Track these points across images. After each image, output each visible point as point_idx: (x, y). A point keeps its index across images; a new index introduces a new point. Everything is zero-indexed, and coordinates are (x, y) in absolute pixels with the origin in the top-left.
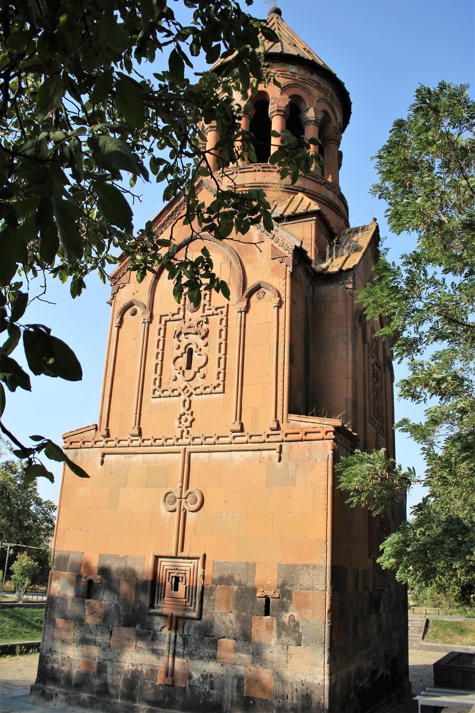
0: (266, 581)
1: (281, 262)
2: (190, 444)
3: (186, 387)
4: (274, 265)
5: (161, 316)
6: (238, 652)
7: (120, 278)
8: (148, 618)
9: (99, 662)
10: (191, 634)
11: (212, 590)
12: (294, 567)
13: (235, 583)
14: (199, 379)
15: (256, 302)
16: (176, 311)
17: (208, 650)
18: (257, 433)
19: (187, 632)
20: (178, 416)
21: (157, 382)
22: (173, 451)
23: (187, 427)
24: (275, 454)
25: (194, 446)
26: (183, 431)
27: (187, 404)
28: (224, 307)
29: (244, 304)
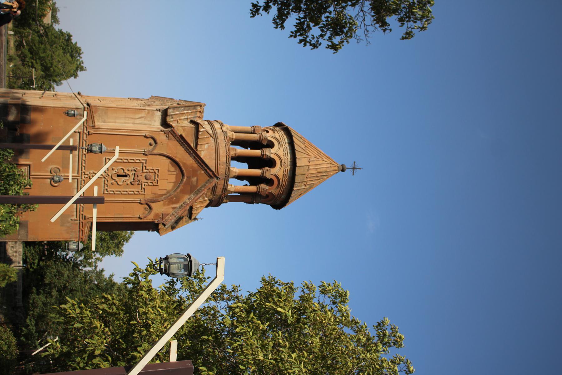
12: (27, 227)
16: (147, 168)
24: (74, 218)
29: (143, 202)
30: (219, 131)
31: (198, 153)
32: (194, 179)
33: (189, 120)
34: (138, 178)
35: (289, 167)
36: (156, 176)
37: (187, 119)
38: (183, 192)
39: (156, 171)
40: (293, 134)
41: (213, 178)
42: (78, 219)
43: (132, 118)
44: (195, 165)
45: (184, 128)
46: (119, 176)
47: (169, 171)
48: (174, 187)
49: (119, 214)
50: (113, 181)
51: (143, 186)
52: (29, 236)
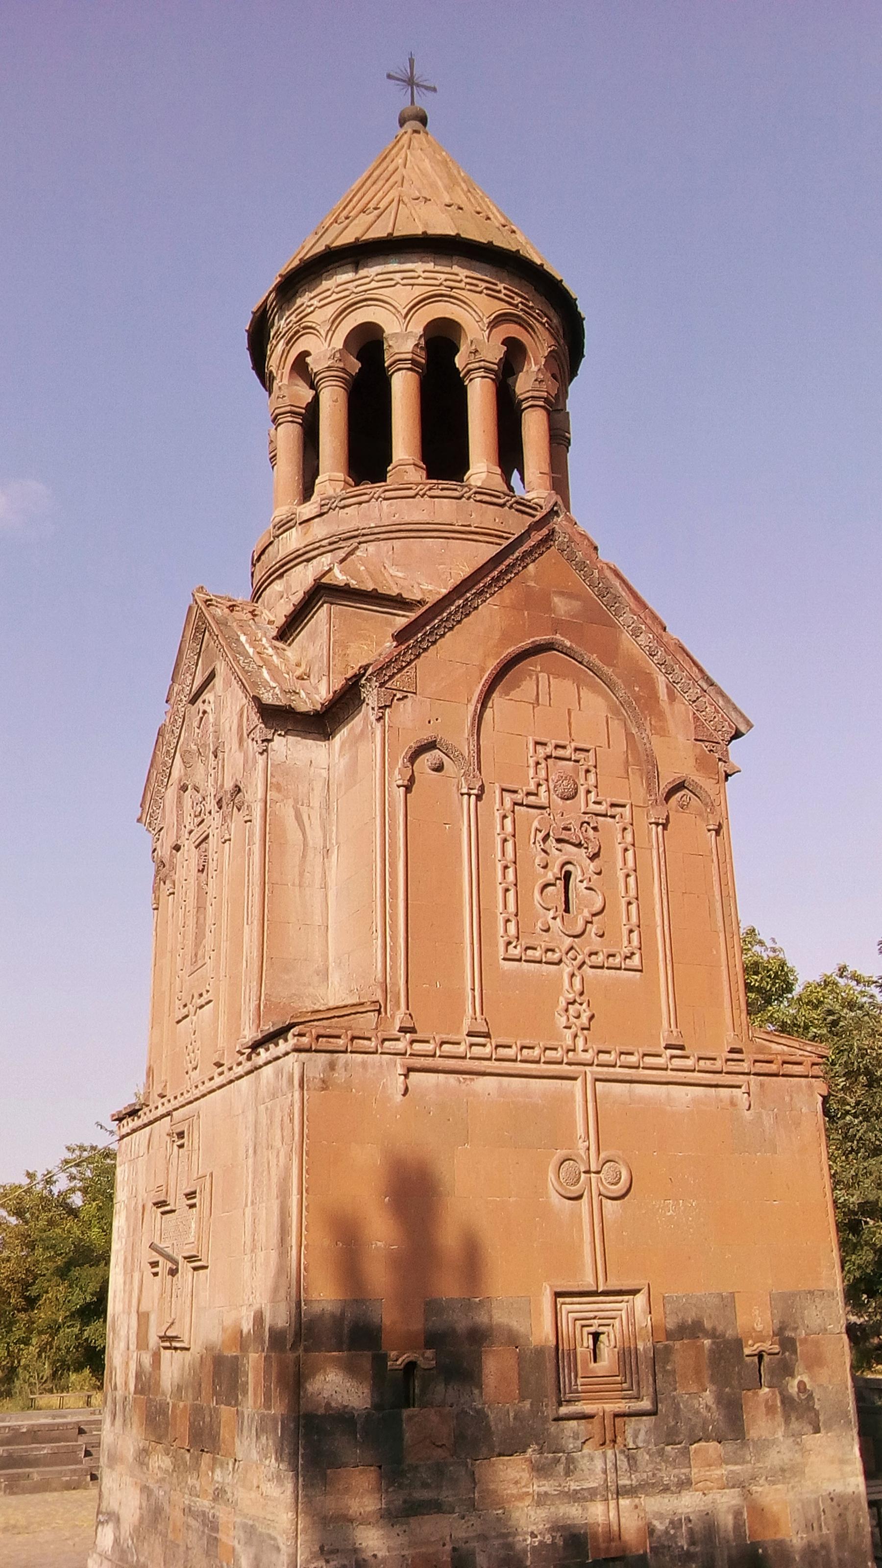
0: (755, 1322)
1: (710, 751)
2: (591, 1065)
3: (572, 948)
4: (698, 751)
5: (503, 790)
6: (727, 1464)
8: (553, 1428)
9: (454, 1549)
10: (640, 1445)
11: (668, 1350)
12: (793, 1295)
13: (707, 1334)
14: (593, 935)
17: (676, 1471)
19: (634, 1442)
20: (564, 1004)
21: (512, 928)
23: (583, 1029)
25: (600, 1069)
27: (577, 981)
28: (624, 806)
30: (319, 530)
31: (432, 600)
34: (575, 826)
35: (456, 269)
36: (560, 753)
37: (275, 648)
38: (610, 653)
40: (320, 248)
41: (553, 531)
43: (304, 856)
44: (507, 594)
45: (337, 647)
46: (567, 910)
50: (593, 929)
51: (601, 809)
52: (825, 1286)
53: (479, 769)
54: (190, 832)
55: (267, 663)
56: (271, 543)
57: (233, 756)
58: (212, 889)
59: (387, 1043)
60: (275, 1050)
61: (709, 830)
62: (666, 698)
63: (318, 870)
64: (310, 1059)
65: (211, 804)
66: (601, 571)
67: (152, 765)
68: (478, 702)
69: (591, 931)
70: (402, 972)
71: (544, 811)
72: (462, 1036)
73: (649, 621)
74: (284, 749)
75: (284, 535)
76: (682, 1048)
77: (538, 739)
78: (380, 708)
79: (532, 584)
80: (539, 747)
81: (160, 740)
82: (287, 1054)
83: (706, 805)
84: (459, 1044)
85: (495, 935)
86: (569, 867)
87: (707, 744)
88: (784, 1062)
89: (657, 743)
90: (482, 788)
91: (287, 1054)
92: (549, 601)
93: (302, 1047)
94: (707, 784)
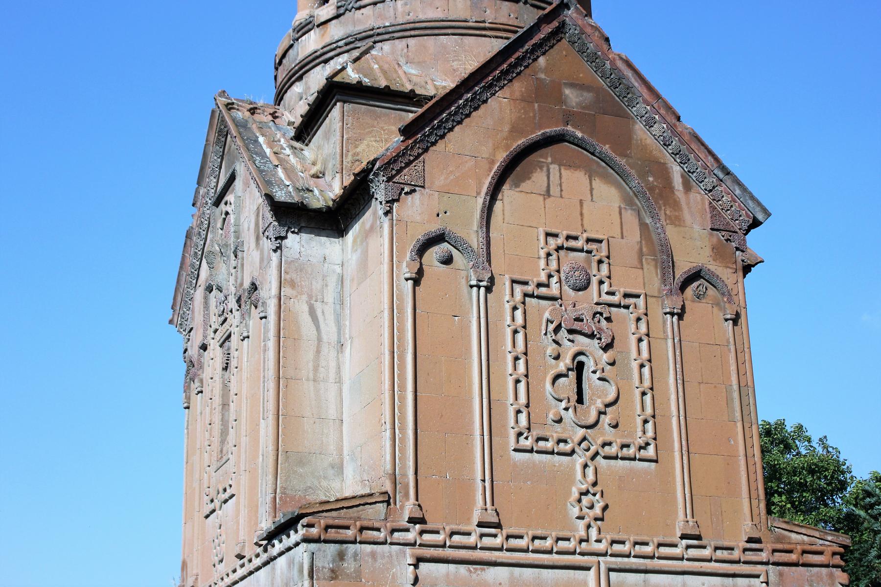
1: (727, 240)
4: (715, 240)
5: (513, 282)
7: (402, 169)
14: (607, 427)
15: (693, 301)
18: (726, 544)
20: (576, 495)
21: (523, 418)
22: (577, 564)
23: (596, 519)
25: (613, 559)
26: (589, 526)
27: (590, 471)
28: (638, 296)
30: (336, 31)
32: (572, 97)
33: (298, 145)
34: (587, 317)
36: (572, 243)
37: (292, 147)
38: (624, 142)
39: (553, 243)
41: (563, 24)
42: (759, 569)
43: (318, 351)
44: (518, 87)
46: (580, 400)
47: (548, 194)
48: (605, 178)
49: (729, 400)
50: (606, 420)
51: (615, 299)
53: (489, 261)
54: (216, 331)
55: (283, 163)
56: (291, 46)
57: (251, 255)
58: (233, 387)
59: (396, 534)
60: (287, 542)
61: (726, 320)
62: (681, 188)
63: (333, 364)
64: (319, 550)
65: (232, 304)
66: (613, 63)
67: (181, 268)
68: (487, 194)
69: (604, 421)
70: (411, 463)
71: (556, 303)
72: (472, 527)
73: (662, 111)
74: (297, 247)
75: (303, 38)
76: (698, 537)
77: (549, 230)
78: (387, 202)
79: (542, 76)
80: (551, 240)
81: (188, 243)
82: (297, 544)
83: (723, 294)
84: (469, 534)
85: (504, 426)
86: (581, 358)
87: (723, 233)
88: (804, 552)
89: (672, 233)
90: (492, 280)
91: (297, 544)
92: (560, 93)
93: (311, 537)
94: (726, 274)
